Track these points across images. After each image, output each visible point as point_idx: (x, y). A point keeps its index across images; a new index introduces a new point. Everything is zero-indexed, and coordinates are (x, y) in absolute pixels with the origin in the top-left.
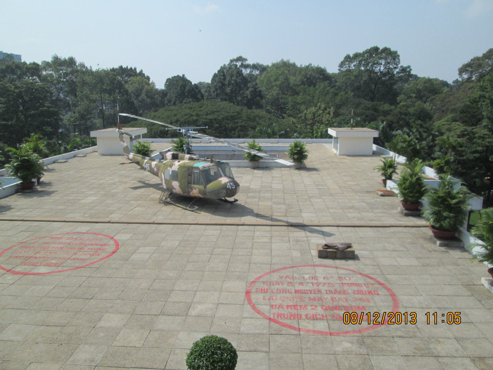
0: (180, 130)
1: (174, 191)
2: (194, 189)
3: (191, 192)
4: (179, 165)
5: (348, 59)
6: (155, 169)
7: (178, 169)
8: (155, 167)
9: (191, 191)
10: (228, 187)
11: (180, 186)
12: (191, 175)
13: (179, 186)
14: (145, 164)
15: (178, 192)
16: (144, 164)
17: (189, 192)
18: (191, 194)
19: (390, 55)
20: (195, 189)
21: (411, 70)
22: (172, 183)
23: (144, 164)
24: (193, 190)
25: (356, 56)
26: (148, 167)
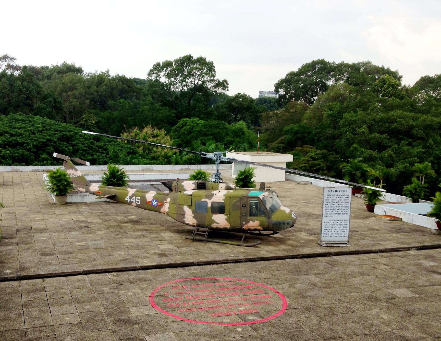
0: (205, 155)
1: (214, 226)
2: (251, 222)
3: (245, 225)
4: (224, 195)
5: (158, 68)
6: (155, 203)
7: (223, 200)
8: (153, 200)
9: (246, 224)
10: (293, 217)
11: (228, 220)
12: (246, 206)
13: (226, 219)
14: (131, 197)
15: (222, 227)
16: (128, 197)
17: (244, 225)
18: (244, 228)
19: (207, 66)
20: (254, 221)
21: (228, 84)
22: (212, 216)
23: (128, 197)
24: (249, 222)
25: (168, 64)
26: (139, 200)
